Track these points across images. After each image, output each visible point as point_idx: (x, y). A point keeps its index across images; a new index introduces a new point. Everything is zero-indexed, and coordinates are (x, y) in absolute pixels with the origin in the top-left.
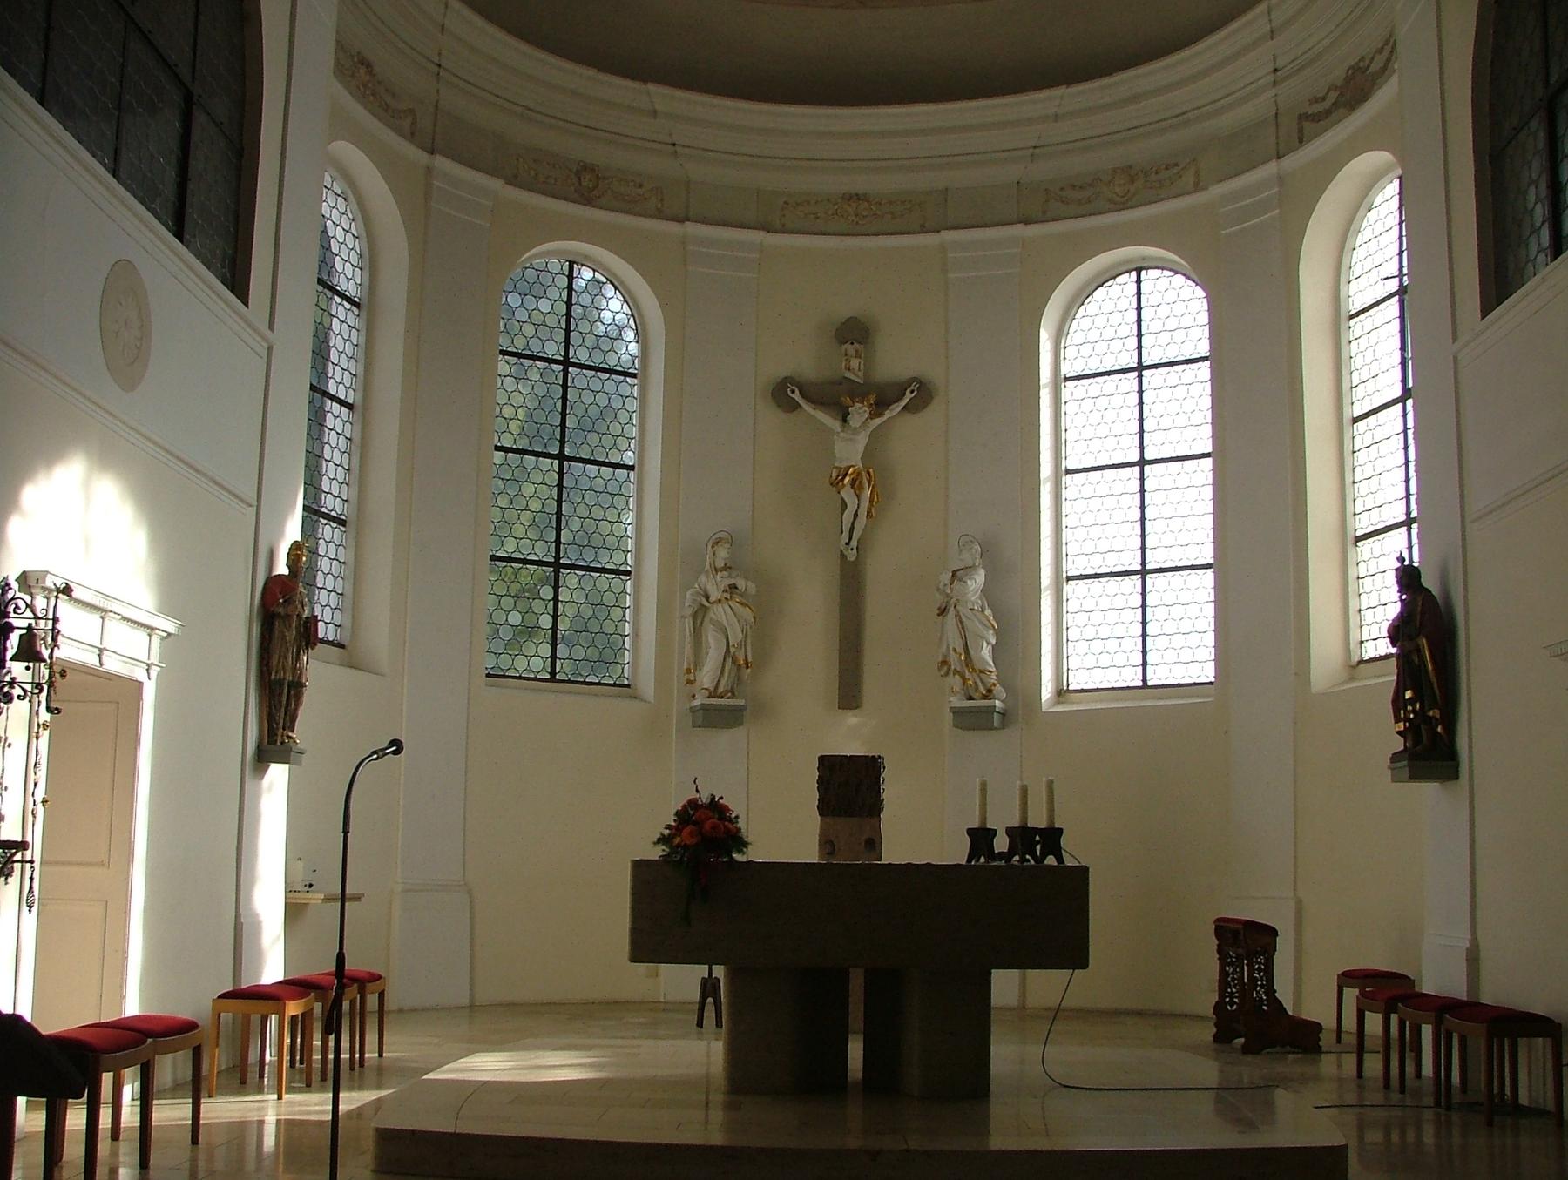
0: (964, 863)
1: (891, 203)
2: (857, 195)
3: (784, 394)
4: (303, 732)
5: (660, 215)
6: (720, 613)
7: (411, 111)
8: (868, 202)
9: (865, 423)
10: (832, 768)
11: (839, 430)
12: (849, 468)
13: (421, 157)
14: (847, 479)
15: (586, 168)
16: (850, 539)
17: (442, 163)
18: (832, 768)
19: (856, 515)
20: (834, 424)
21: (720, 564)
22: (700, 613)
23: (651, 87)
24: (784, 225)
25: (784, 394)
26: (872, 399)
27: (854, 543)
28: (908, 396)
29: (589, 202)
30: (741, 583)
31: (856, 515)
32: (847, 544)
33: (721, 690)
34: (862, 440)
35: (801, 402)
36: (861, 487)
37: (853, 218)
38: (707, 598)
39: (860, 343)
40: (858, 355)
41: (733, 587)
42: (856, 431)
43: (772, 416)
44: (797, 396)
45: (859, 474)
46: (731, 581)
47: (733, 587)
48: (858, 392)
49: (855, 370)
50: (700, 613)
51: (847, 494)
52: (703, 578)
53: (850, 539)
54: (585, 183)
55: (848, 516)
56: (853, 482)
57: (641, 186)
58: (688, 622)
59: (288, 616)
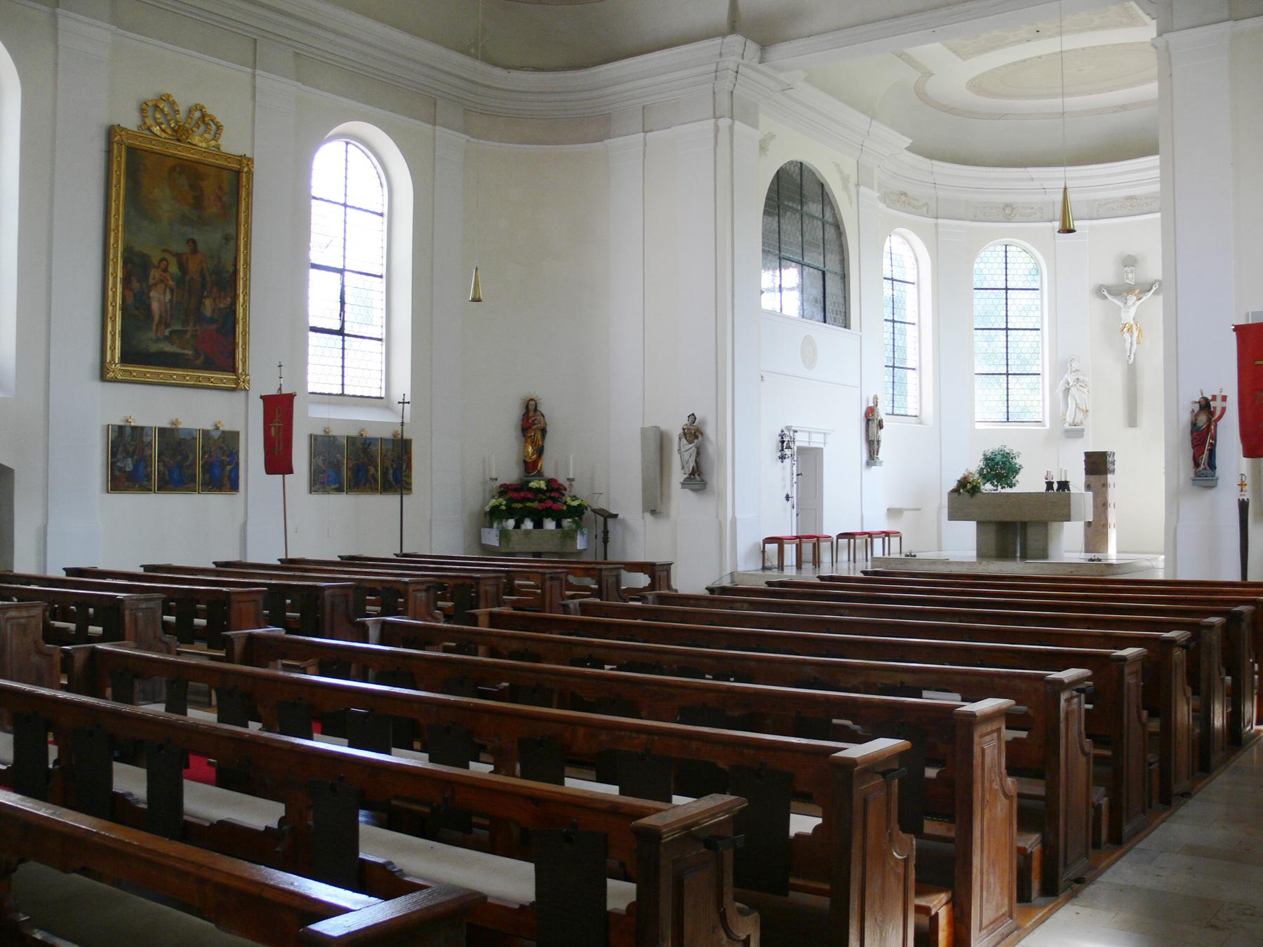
0: (1044, 491)
1: (1146, 198)
2: (1131, 196)
3: (1101, 291)
4: (882, 455)
5: (1042, 220)
6: (1073, 390)
7: (926, 204)
8: (1136, 199)
9: (1134, 304)
10: (1088, 455)
11: (1122, 307)
12: (1126, 324)
13: (934, 221)
14: (1125, 330)
15: (1007, 205)
16: (1130, 353)
17: (940, 221)
18: (1088, 455)
19: (1131, 344)
20: (1121, 305)
21: (1074, 369)
22: (1067, 391)
23: (1029, 169)
24: (1098, 215)
25: (1101, 291)
26: (1137, 292)
27: (1132, 356)
28: (1154, 289)
29: (1009, 221)
30: (1081, 378)
31: (1131, 344)
32: (1129, 356)
33: (1076, 421)
34: (1133, 311)
35: (1108, 296)
36: (1132, 332)
37: (1130, 208)
38: (1068, 384)
39: (1132, 266)
40: (1132, 272)
41: (1078, 379)
42: (1129, 307)
43: (1098, 302)
44: (1105, 293)
45: (1131, 326)
46: (1076, 377)
47: (1078, 379)
48: (1129, 290)
49: (1130, 279)
50: (1067, 391)
51: (1127, 336)
52: (1066, 376)
53: (1130, 353)
54: (1007, 212)
55: (1128, 345)
56: (1129, 329)
57: (1032, 208)
58: (1061, 396)
59: (874, 420)
